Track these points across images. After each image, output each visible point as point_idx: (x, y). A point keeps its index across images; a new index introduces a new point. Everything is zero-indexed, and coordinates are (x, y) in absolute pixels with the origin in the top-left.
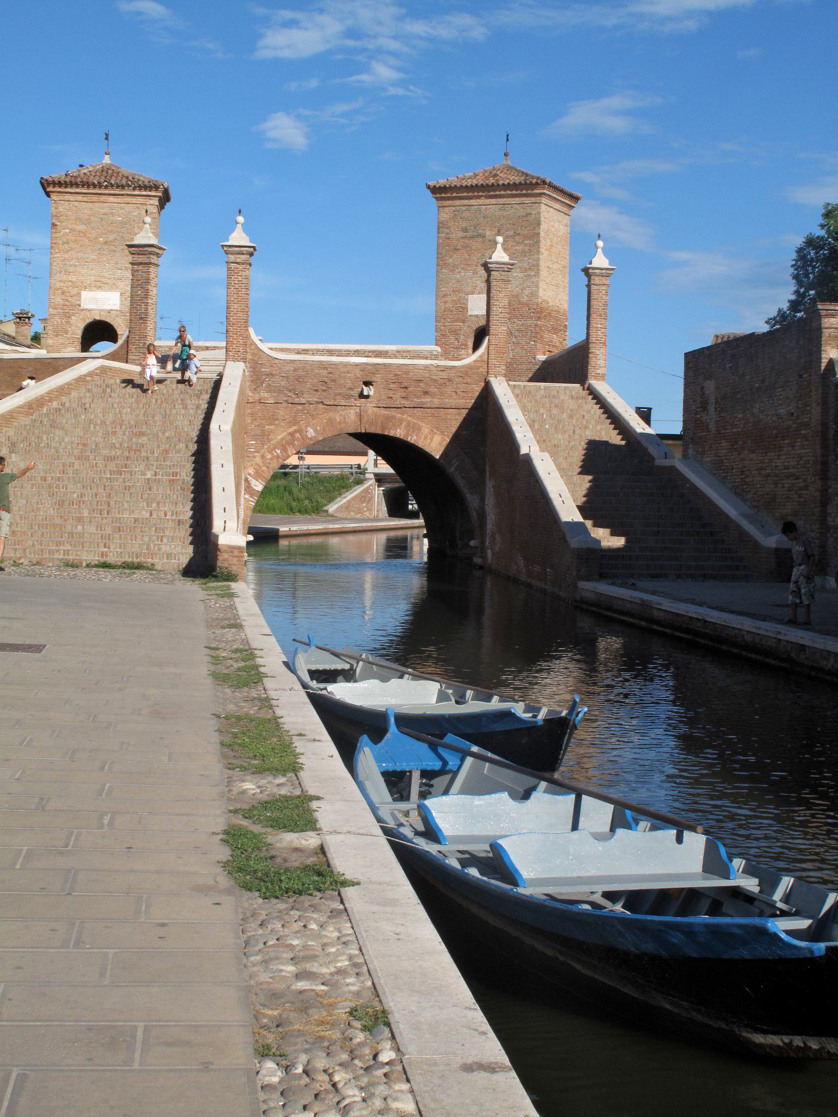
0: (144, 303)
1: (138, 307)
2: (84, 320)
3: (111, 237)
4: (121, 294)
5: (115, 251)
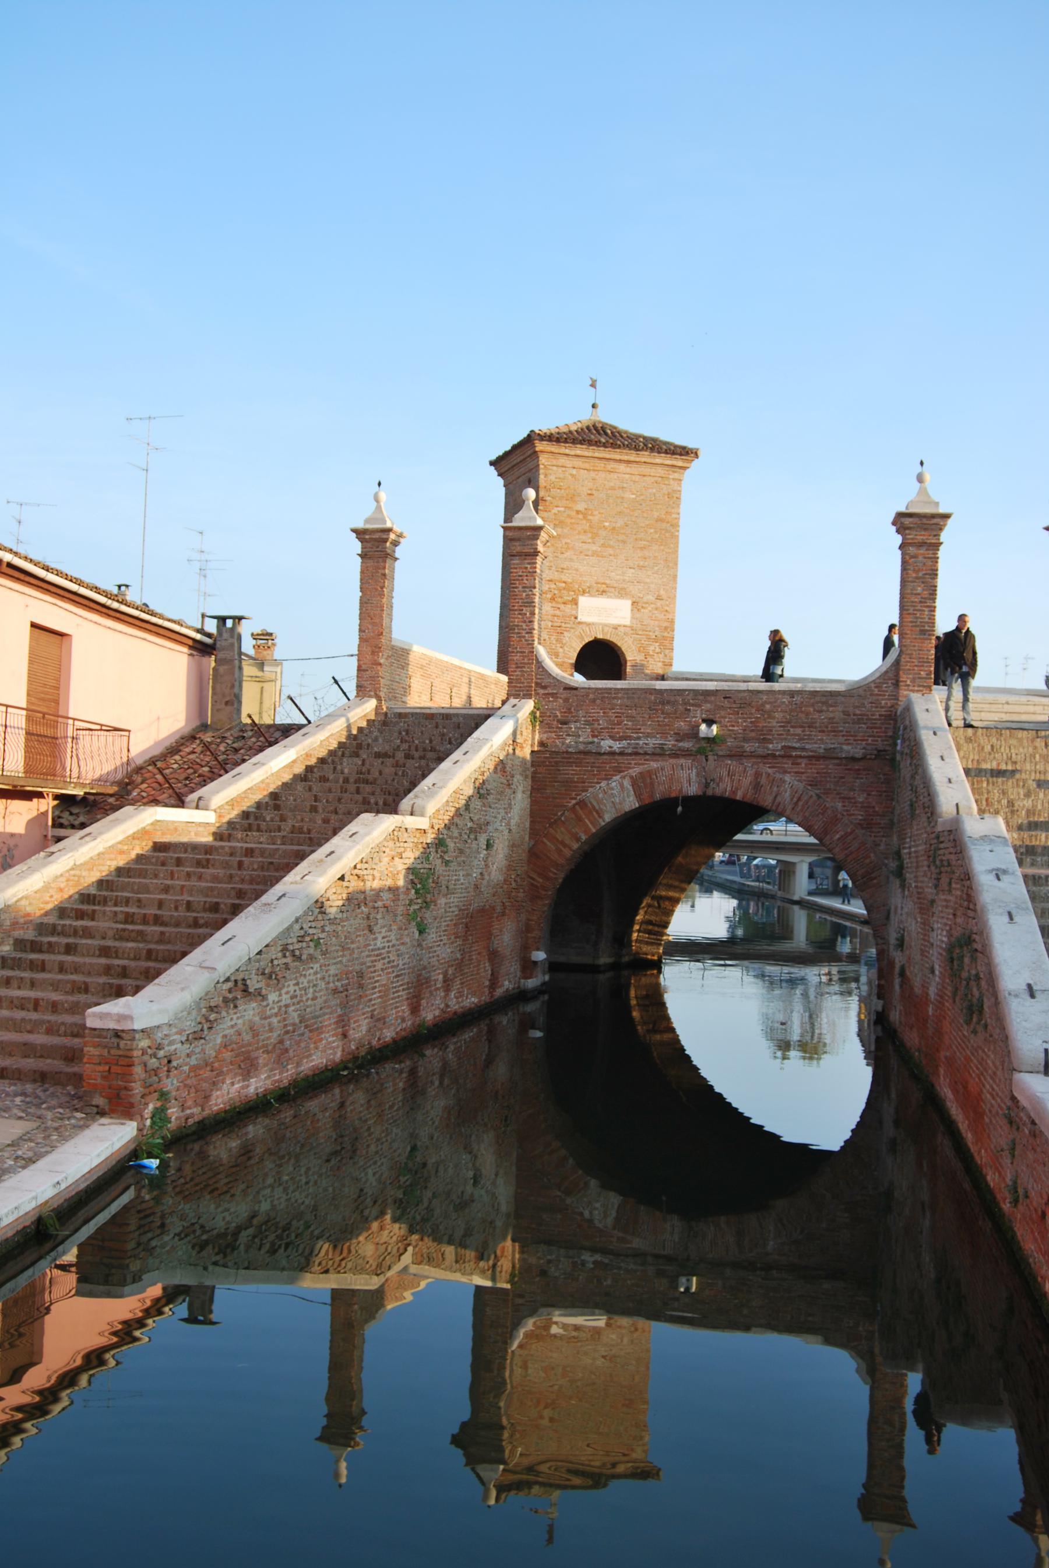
0: (928, 607)
2: (581, 638)
3: (620, 523)
4: (633, 603)
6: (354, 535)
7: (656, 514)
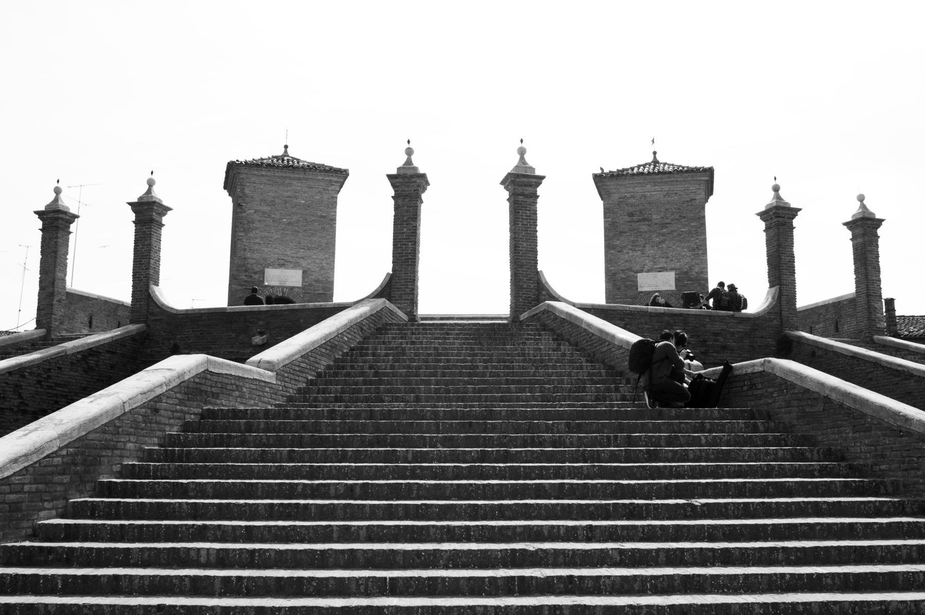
1: (404, 246)
3: (295, 218)
4: (304, 272)
5: (296, 231)
6: (37, 216)
7: (319, 213)
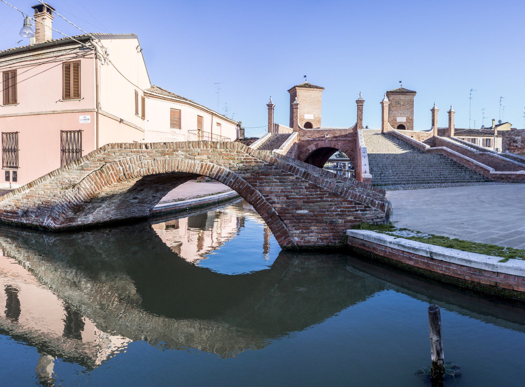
3: (311, 101)
4: (314, 115)
